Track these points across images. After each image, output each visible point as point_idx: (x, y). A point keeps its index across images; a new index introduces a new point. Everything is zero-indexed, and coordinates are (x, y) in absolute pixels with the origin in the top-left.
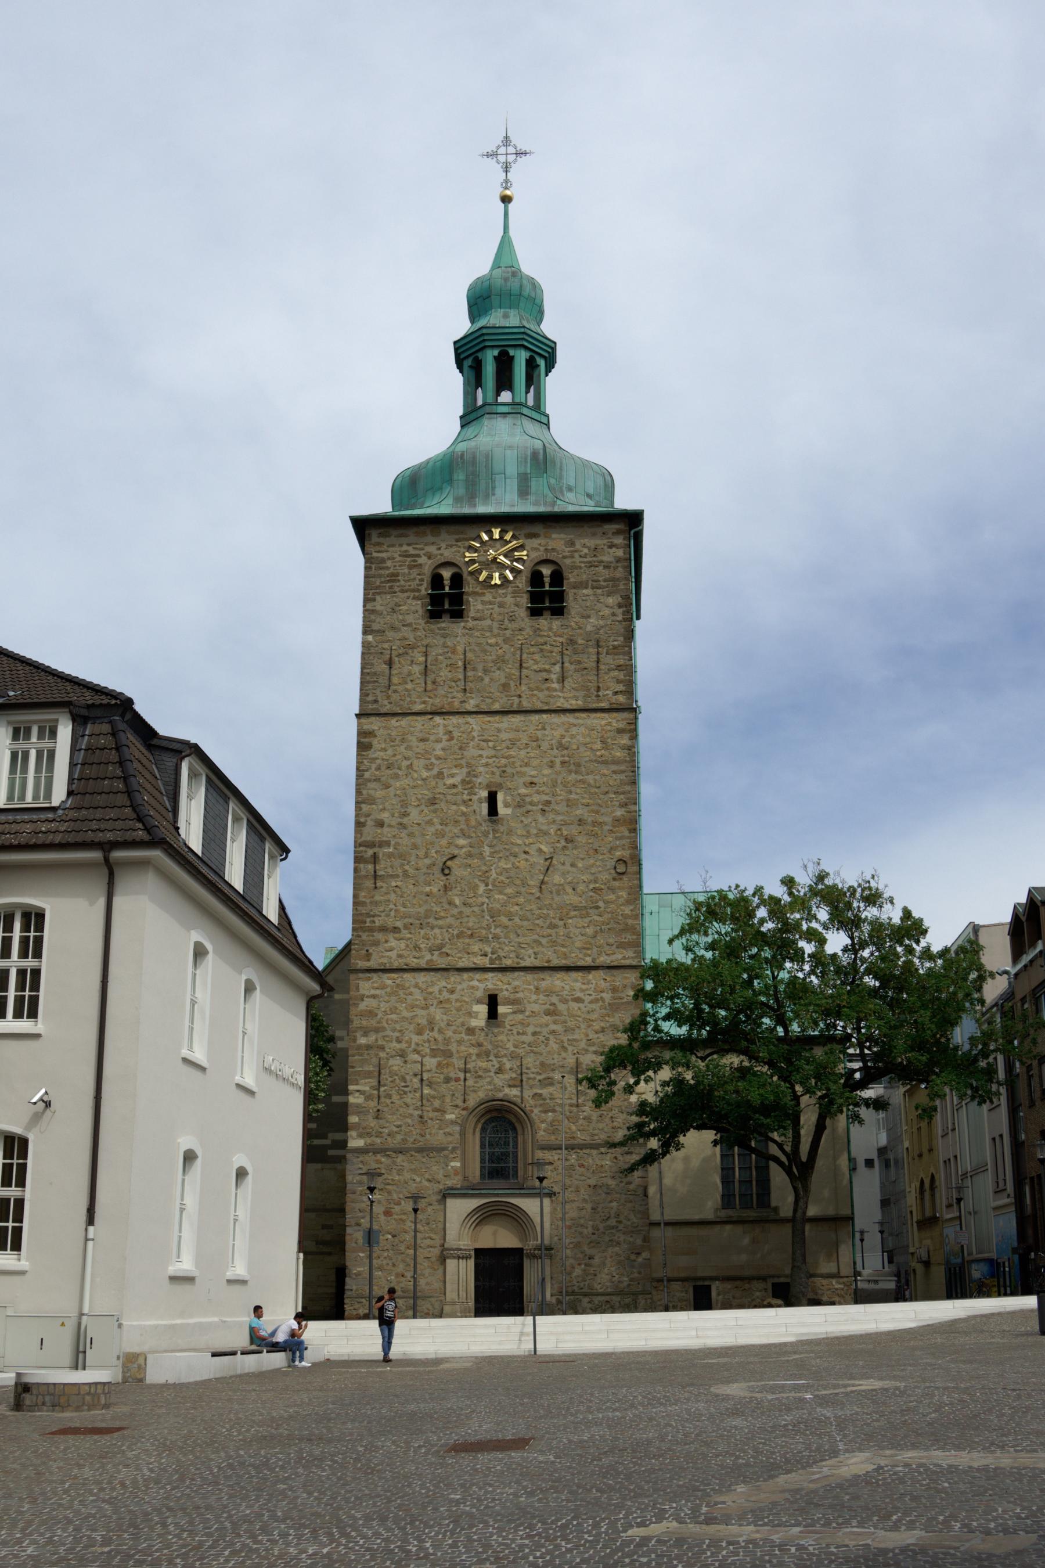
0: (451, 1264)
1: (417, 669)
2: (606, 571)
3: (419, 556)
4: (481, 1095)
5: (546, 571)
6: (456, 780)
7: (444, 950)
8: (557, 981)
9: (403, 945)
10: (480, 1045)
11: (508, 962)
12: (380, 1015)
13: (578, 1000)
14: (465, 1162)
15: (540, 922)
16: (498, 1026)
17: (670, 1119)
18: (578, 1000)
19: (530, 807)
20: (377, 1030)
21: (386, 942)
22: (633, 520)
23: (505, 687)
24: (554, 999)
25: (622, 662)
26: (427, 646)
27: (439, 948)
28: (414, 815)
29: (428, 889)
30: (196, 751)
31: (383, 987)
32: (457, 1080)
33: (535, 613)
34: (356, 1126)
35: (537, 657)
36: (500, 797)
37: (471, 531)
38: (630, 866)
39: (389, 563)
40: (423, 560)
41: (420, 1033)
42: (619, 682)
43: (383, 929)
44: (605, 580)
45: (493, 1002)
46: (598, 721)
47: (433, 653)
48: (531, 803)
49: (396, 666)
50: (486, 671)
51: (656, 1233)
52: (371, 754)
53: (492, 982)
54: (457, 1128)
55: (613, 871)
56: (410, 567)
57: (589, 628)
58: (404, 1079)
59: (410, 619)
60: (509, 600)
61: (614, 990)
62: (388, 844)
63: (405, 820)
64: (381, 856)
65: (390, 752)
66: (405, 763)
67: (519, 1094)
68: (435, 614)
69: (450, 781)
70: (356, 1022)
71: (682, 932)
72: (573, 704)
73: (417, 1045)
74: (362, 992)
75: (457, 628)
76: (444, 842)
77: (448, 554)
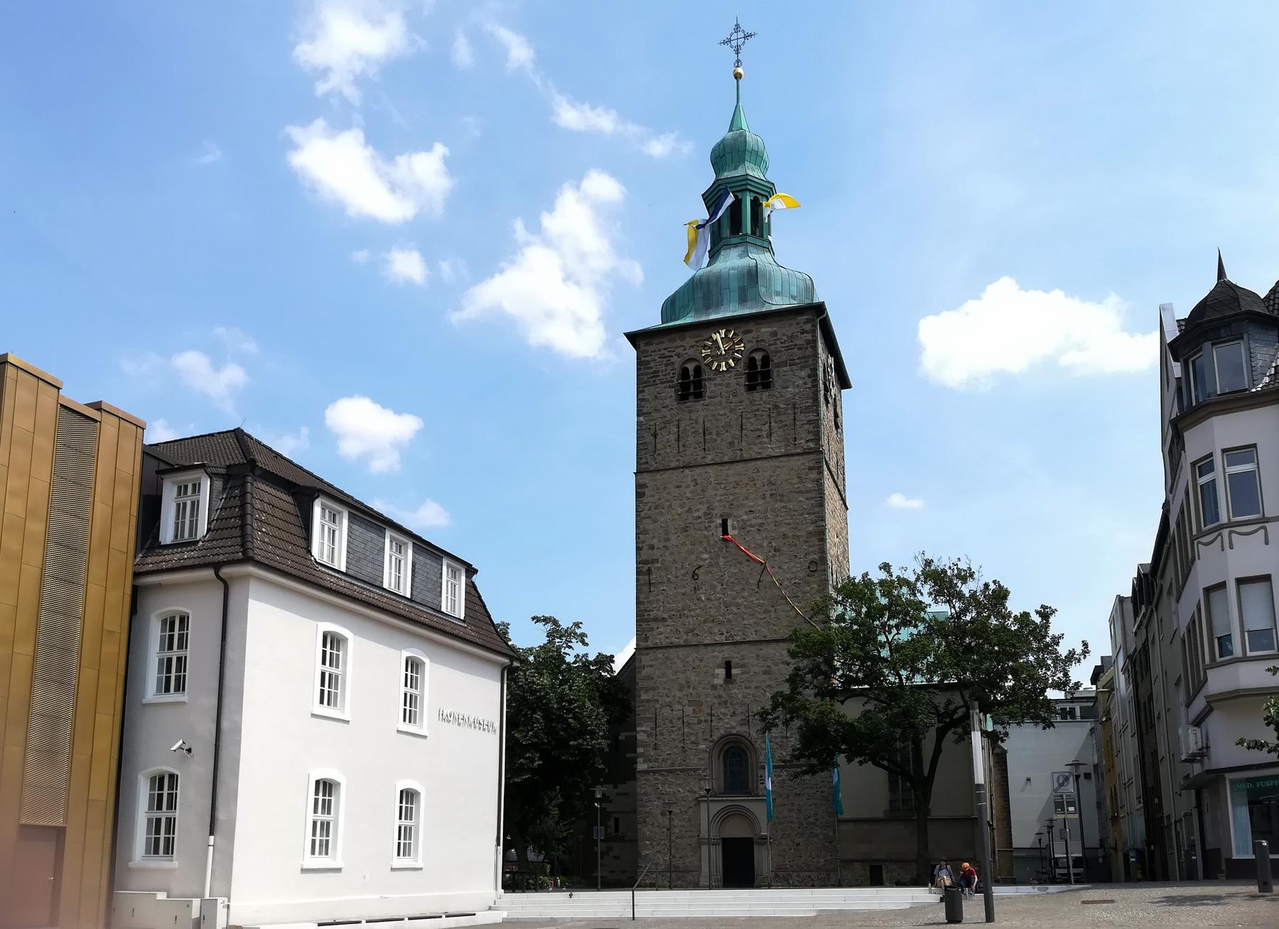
1: (673, 437)
4: (722, 731)
6: (700, 513)
11: (738, 638)
20: (654, 689)
23: (731, 444)
24: (769, 663)
33: (751, 388)
34: (642, 755)
35: (752, 420)
41: (681, 690)
43: (656, 620)
45: (728, 666)
48: (751, 526)
50: (718, 434)
53: (727, 652)
56: (666, 365)
57: (788, 396)
58: (671, 722)
59: (667, 402)
60: (733, 381)
63: (668, 544)
68: (683, 398)
69: (696, 515)
75: (699, 405)
76: (693, 557)
77: (691, 352)
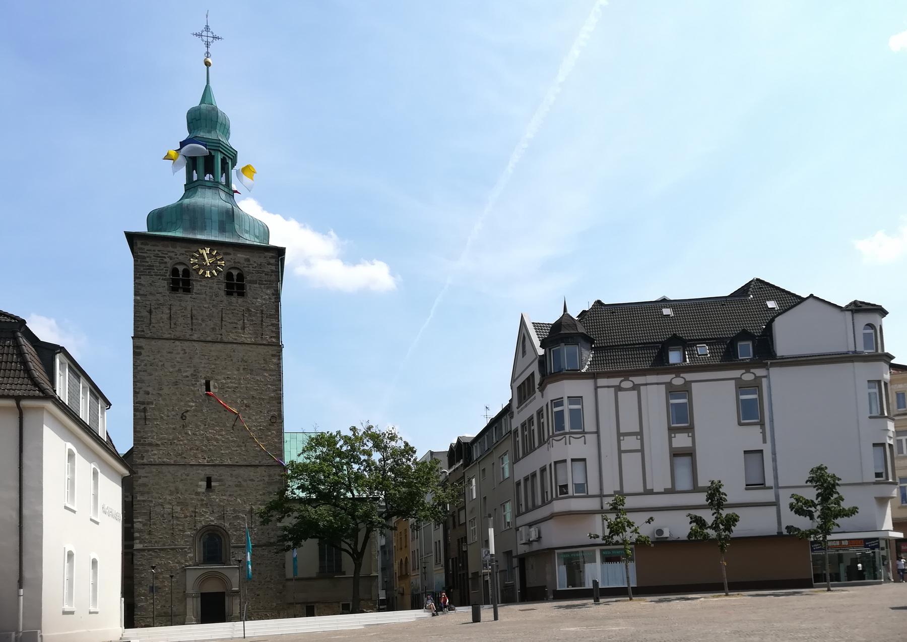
1: (165, 317)
8: (241, 471)
10: (203, 500)
11: (217, 462)
14: (194, 554)
17: (299, 534)
20: (148, 493)
23: (213, 329)
24: (240, 480)
28: (166, 390)
30: (62, 350)
31: (151, 472)
33: (229, 294)
36: (212, 383)
37: (194, 248)
38: (277, 419)
39: (148, 259)
40: (167, 260)
43: (150, 444)
45: (209, 480)
46: (262, 350)
47: (174, 309)
48: (228, 387)
49: (154, 313)
50: (203, 320)
51: (289, 583)
52: (141, 358)
53: (208, 471)
54: (191, 539)
58: (163, 516)
59: (160, 290)
61: (270, 476)
65: (152, 357)
66: (160, 364)
68: (174, 289)
70: (137, 489)
71: (304, 451)
72: (249, 341)
75: (188, 297)
77: (181, 258)
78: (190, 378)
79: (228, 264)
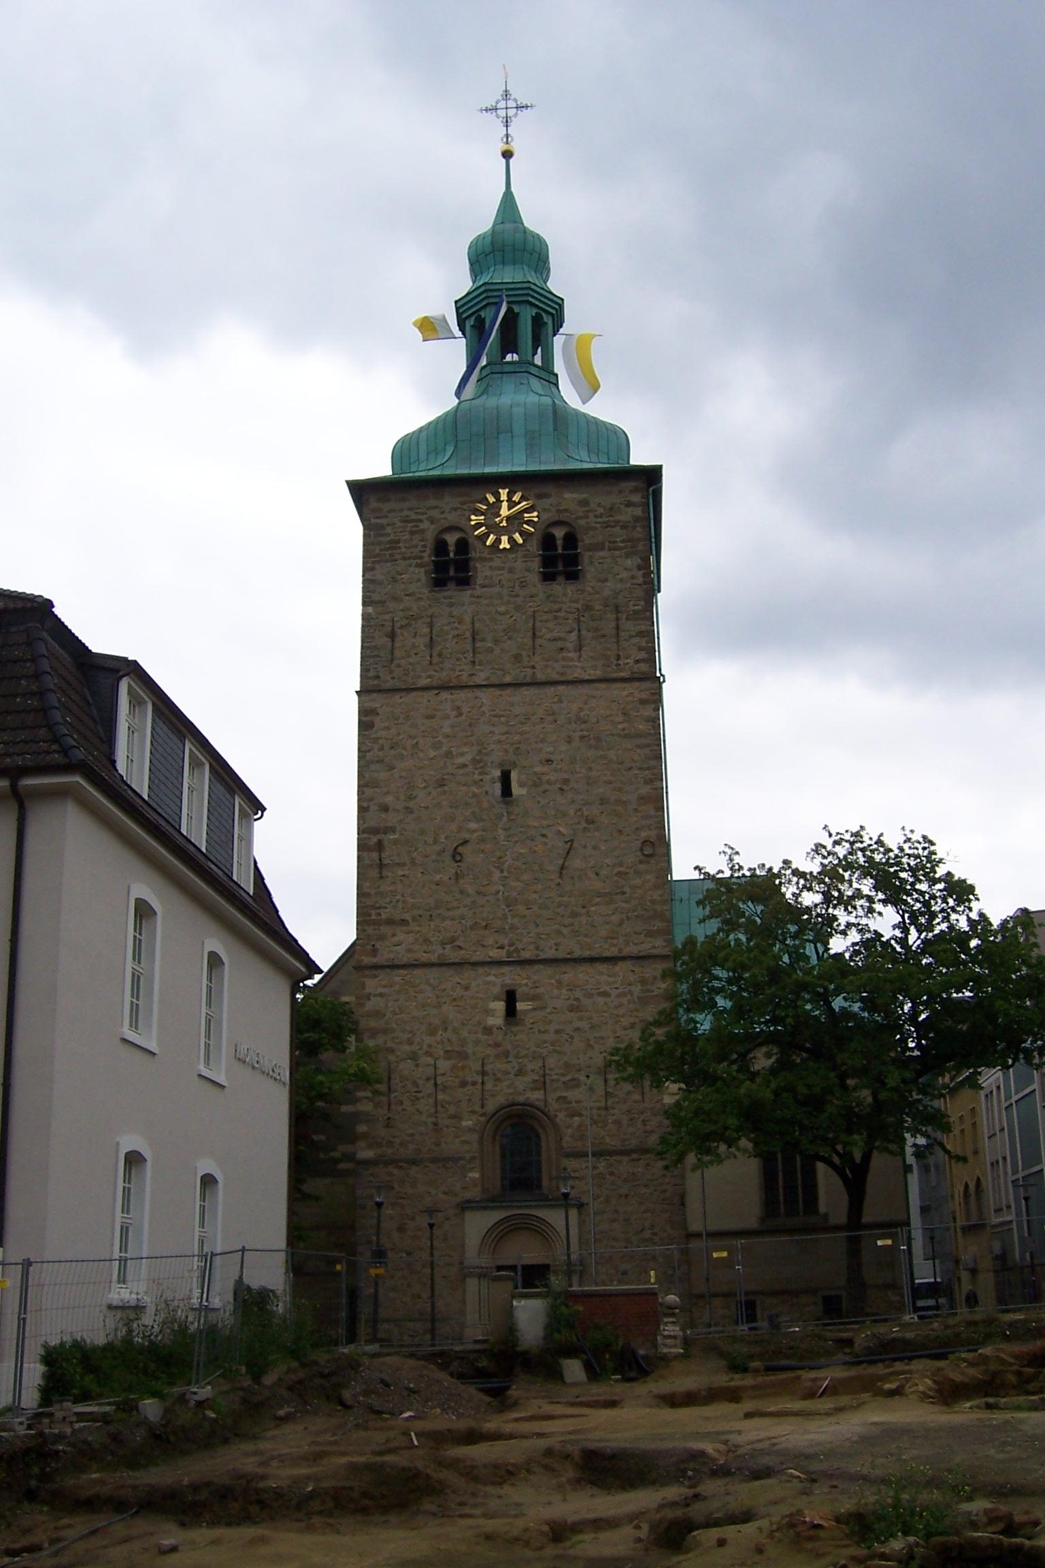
0: (472, 1284)
1: (421, 641)
2: (624, 531)
3: (420, 521)
4: (501, 1100)
5: (559, 533)
6: (467, 759)
7: (457, 943)
9: (411, 938)
11: (526, 955)
12: (388, 1015)
13: (605, 994)
15: (561, 910)
16: (517, 1024)
18: (605, 994)
19: (547, 787)
20: (385, 1031)
21: (394, 935)
22: (651, 477)
23: (517, 658)
24: (578, 994)
25: (643, 628)
26: (431, 617)
27: (453, 940)
29: (438, 877)
32: (474, 1083)
33: (548, 577)
34: (364, 1136)
35: (551, 625)
39: (389, 530)
41: (432, 1032)
42: (640, 649)
43: (390, 922)
44: (622, 542)
45: (511, 998)
48: (549, 782)
49: (399, 639)
50: (496, 641)
54: (474, 1137)
55: (639, 853)
56: (412, 533)
57: (607, 592)
58: (415, 1084)
59: (412, 588)
60: (519, 565)
61: (643, 982)
62: (392, 830)
63: (411, 804)
64: (386, 843)
66: (410, 742)
67: (542, 1097)
68: (439, 583)
69: (460, 760)
73: (430, 1046)
74: (368, 990)
75: (465, 595)
76: (453, 827)
77: (453, 518)
78: (470, 768)
79: (545, 516)
